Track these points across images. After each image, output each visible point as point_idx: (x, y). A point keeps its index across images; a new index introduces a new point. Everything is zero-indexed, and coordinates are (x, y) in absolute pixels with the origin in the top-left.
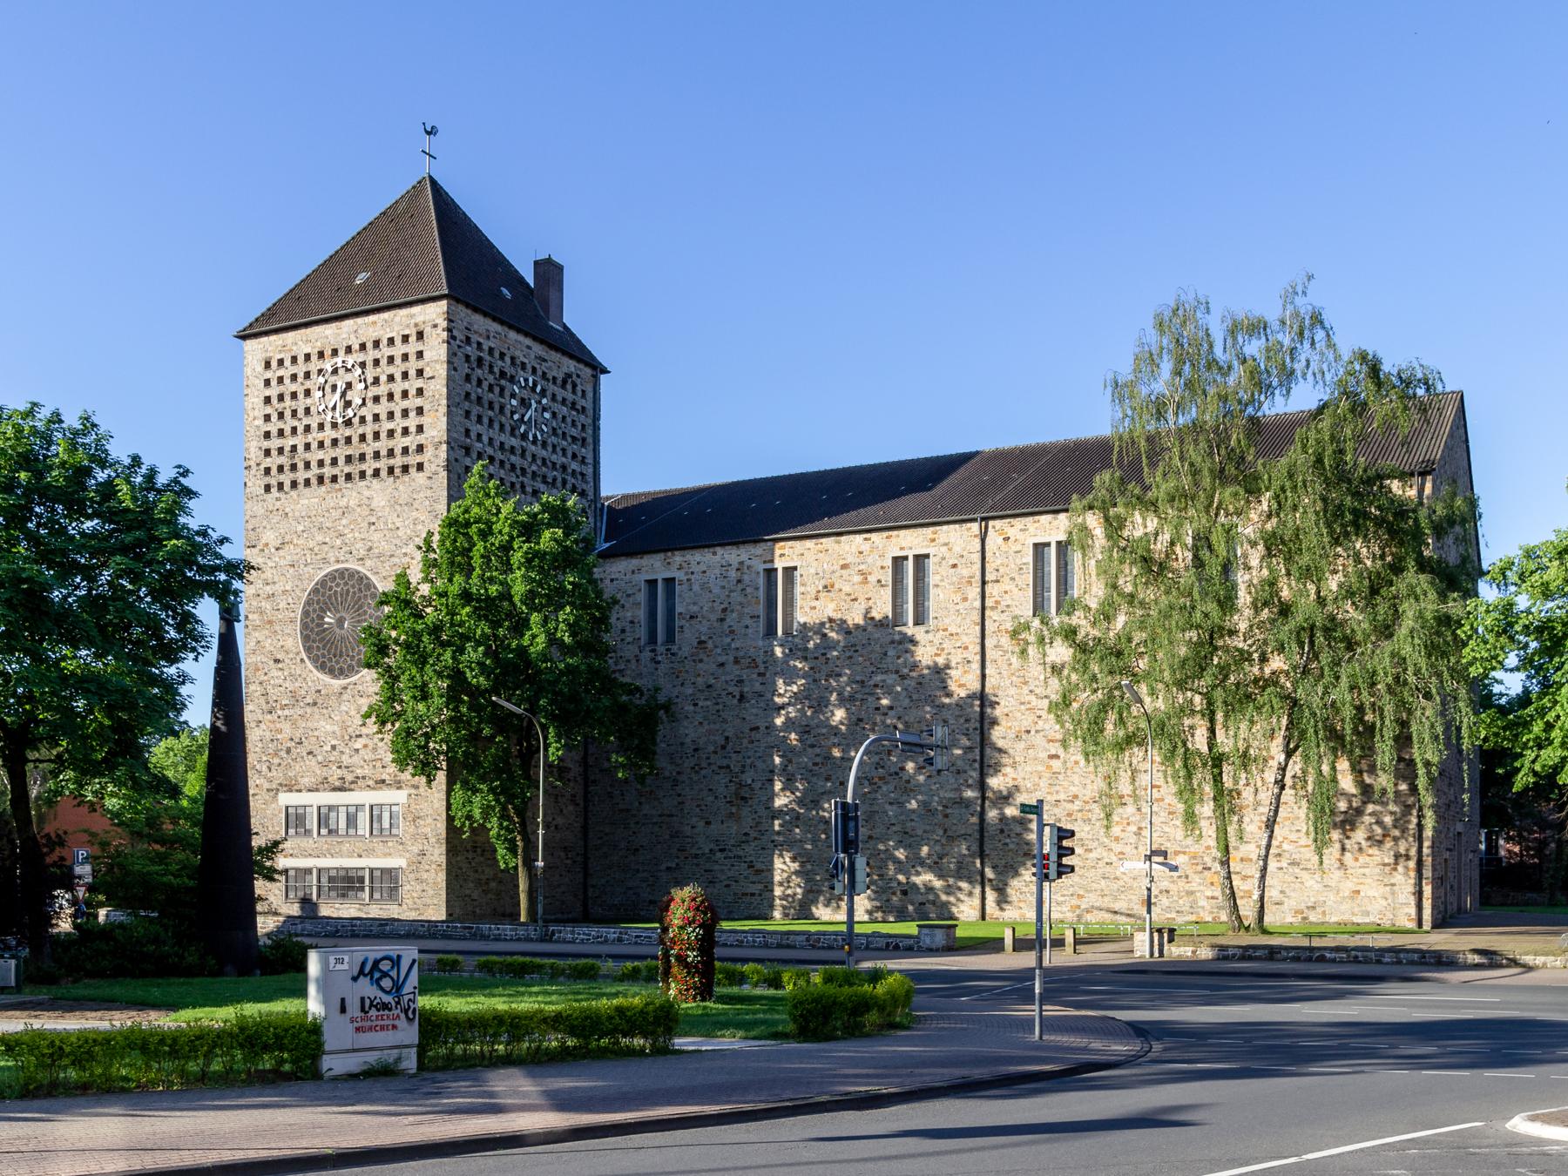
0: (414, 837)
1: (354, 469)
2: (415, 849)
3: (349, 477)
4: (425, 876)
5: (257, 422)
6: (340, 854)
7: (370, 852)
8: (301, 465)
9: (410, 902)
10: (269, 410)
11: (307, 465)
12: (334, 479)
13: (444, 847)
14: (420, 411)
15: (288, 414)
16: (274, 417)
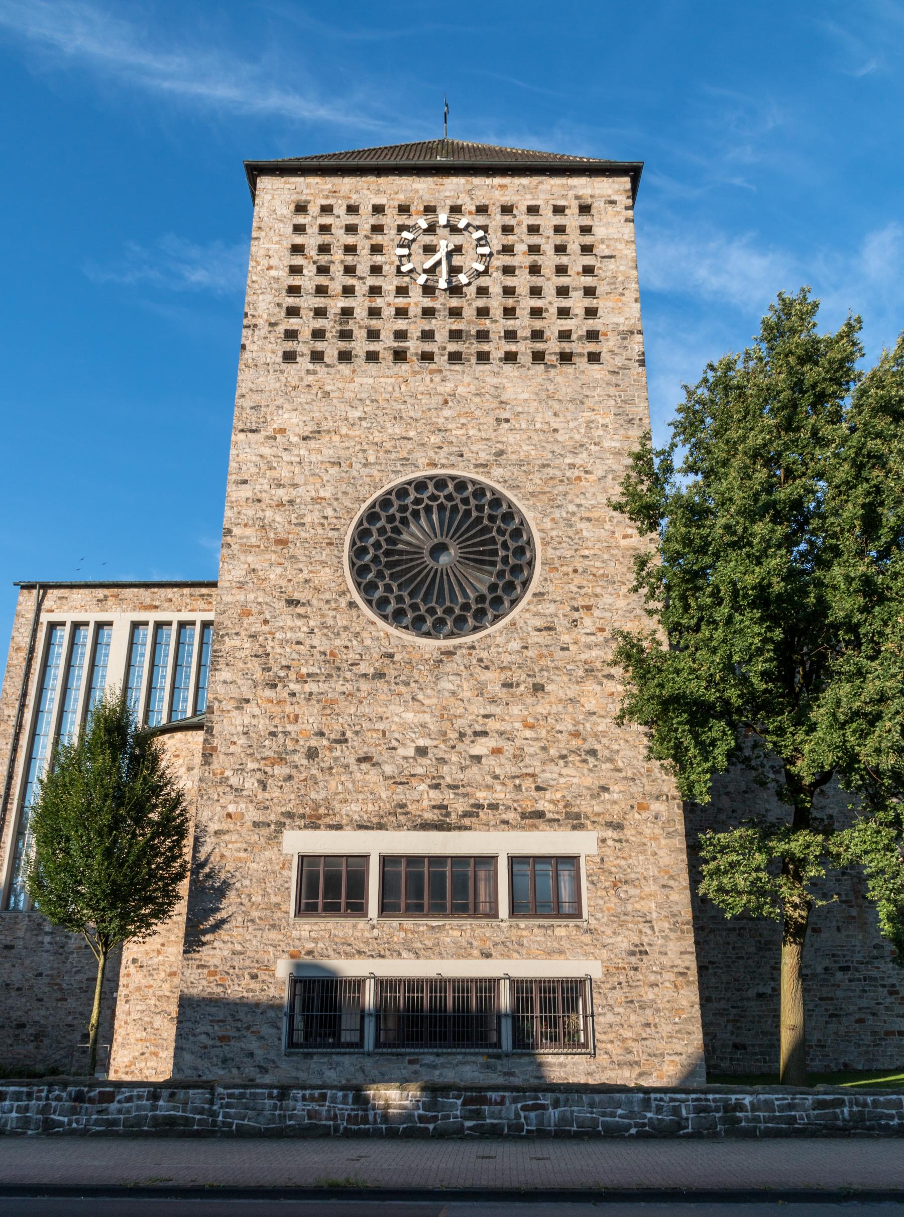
0: (619, 920)
1: (470, 348)
2: (623, 942)
3: (455, 357)
4: (650, 995)
5: (273, 273)
6: (435, 951)
7: (508, 949)
8: (360, 334)
9: (615, 1049)
10: (298, 260)
11: (373, 335)
12: (427, 357)
13: (690, 939)
14: (590, 292)
15: (337, 270)
16: (310, 270)
